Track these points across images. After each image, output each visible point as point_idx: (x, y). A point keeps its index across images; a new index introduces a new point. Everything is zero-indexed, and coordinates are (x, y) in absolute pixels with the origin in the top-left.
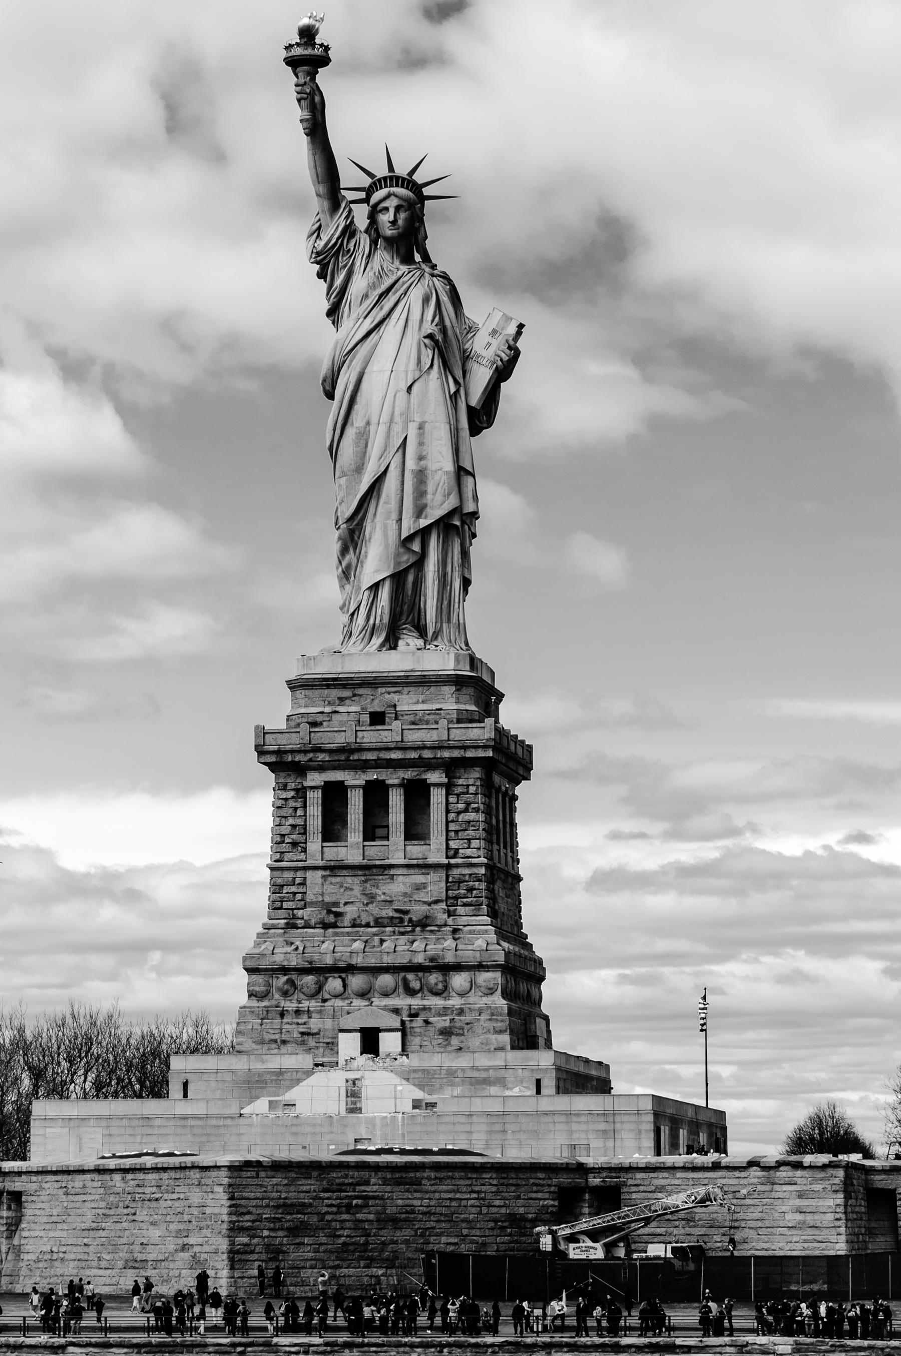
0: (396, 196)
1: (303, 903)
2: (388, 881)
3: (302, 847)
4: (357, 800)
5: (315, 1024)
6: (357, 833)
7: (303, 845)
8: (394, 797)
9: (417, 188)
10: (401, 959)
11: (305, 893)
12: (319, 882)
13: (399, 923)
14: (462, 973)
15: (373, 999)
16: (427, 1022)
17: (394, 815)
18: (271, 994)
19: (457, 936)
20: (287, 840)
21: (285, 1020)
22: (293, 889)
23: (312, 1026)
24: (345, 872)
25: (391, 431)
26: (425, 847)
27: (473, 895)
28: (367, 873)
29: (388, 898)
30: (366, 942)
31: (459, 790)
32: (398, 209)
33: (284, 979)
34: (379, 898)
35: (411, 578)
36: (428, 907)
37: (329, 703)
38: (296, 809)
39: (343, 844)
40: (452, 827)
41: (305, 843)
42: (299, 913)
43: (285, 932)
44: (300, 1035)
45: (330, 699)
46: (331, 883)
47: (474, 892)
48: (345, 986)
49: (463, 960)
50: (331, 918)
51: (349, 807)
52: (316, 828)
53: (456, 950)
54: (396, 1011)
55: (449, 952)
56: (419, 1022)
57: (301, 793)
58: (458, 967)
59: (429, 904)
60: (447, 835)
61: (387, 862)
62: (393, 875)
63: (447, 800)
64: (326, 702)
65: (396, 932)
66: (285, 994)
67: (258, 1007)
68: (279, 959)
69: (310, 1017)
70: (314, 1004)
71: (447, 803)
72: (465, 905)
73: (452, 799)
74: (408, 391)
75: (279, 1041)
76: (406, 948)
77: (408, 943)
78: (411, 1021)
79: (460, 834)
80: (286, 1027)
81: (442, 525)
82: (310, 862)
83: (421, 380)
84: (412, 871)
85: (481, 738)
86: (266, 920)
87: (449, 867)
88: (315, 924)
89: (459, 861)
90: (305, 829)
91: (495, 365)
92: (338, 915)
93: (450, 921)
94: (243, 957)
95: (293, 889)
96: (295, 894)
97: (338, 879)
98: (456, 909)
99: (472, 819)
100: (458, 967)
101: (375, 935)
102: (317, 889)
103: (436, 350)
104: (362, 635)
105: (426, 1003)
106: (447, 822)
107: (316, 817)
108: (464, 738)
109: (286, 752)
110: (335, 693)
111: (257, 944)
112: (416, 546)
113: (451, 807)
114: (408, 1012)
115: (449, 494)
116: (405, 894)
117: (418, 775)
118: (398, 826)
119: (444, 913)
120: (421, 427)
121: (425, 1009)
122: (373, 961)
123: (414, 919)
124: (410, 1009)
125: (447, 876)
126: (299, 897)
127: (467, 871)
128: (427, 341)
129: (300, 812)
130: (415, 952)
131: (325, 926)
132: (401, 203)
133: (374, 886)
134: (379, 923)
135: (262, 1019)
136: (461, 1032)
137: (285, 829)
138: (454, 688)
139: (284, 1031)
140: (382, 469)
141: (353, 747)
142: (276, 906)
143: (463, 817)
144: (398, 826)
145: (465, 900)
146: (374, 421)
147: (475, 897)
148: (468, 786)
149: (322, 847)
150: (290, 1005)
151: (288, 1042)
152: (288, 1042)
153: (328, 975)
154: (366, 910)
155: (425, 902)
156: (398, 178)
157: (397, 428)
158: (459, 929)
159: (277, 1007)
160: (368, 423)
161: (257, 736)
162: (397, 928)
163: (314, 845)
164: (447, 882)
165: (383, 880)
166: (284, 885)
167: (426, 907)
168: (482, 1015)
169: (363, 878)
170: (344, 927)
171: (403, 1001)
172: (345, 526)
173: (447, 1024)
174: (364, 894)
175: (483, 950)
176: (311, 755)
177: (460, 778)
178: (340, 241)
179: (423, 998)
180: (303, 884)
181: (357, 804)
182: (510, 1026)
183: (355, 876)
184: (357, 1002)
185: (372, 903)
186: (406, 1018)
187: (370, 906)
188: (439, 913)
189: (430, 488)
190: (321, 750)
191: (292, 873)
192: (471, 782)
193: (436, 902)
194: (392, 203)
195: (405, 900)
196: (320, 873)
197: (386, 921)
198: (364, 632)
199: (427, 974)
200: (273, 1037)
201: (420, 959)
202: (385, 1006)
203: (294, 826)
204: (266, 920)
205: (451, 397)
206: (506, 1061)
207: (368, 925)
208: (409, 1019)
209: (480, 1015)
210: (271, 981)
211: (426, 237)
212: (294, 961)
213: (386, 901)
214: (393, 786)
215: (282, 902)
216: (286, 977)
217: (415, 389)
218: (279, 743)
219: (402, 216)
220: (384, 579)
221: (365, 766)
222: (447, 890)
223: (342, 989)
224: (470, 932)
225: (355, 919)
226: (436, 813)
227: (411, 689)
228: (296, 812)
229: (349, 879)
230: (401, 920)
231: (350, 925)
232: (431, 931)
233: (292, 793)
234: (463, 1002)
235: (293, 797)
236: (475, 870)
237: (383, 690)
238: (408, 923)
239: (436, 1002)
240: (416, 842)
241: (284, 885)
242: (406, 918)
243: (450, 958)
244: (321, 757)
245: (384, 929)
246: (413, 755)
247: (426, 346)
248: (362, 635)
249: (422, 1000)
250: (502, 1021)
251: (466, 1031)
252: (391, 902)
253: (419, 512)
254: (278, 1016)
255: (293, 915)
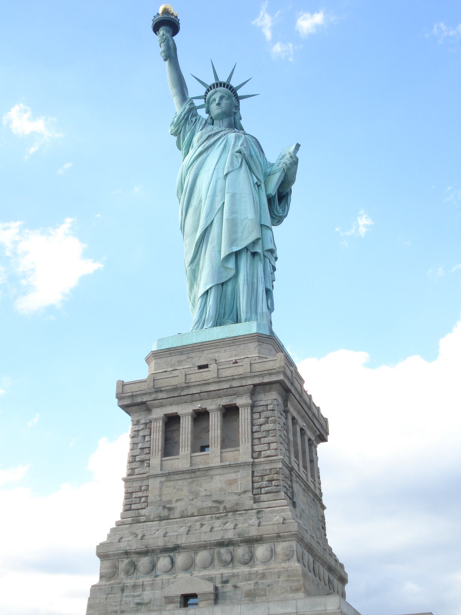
0: (220, 91)
1: (146, 504)
2: (209, 480)
3: (148, 463)
4: (187, 424)
5: (147, 595)
6: (186, 448)
7: (147, 461)
8: (213, 419)
9: (233, 91)
10: (216, 537)
11: (148, 496)
12: (158, 487)
13: (216, 511)
14: (264, 545)
15: (194, 572)
16: (235, 587)
17: (213, 431)
18: (116, 575)
19: (260, 516)
20: (138, 459)
21: (125, 594)
22: (140, 494)
23: (145, 598)
24: (177, 477)
25: (250, 300)
26: (236, 452)
27: (273, 485)
28: (193, 475)
29: (208, 493)
30: (190, 527)
31: (260, 409)
32: (221, 98)
33: (126, 561)
34: (202, 494)
35: (229, 288)
36: (238, 497)
37: (171, 365)
38: (144, 436)
39: (176, 457)
40: (256, 435)
41: (149, 460)
42: (143, 512)
43: (130, 526)
44: (135, 606)
45: (171, 363)
46: (167, 487)
47: (274, 482)
48: (173, 562)
49: (264, 533)
50: (166, 513)
51: (181, 430)
52: (157, 447)
53: (259, 526)
54: (211, 579)
55: (253, 527)
56: (229, 587)
57: (148, 424)
58: (259, 540)
59: (239, 495)
60: (252, 442)
61: (208, 466)
62: (212, 476)
63: (252, 417)
64: (169, 365)
65: (214, 518)
66: (127, 573)
67: (105, 585)
68: (123, 546)
69: (144, 590)
70: (147, 580)
71: (252, 419)
72: (267, 493)
73: (256, 416)
74: (224, 179)
75: (119, 611)
76: (220, 528)
77: (222, 525)
78: (223, 587)
79: (262, 440)
80: (124, 599)
81: (249, 253)
82: (152, 472)
83: (233, 173)
84: (226, 471)
85: (274, 368)
86: (119, 519)
87: (253, 464)
88: (154, 518)
89: (262, 460)
90: (150, 450)
91: (283, 168)
92: (170, 509)
93: (255, 506)
94: (97, 546)
95: (140, 494)
96: (140, 498)
97: (172, 483)
98: (260, 496)
99: (270, 429)
100: (259, 540)
101: (197, 521)
102: (156, 493)
103: (244, 160)
104: (197, 325)
105: (235, 571)
106: (253, 432)
107: (157, 440)
108: (262, 369)
109: (136, 396)
110: (175, 359)
111: (109, 536)
112: (231, 264)
113: (255, 422)
114: (220, 580)
115: (252, 231)
116: (221, 490)
117: (230, 401)
118: (216, 439)
119: (251, 500)
120: (233, 196)
121: (234, 576)
122: (194, 540)
123: (228, 506)
124: (222, 576)
125: (253, 472)
126: (143, 500)
127: (268, 467)
128: (238, 154)
129: (147, 439)
130: (227, 530)
131: (161, 519)
132: (223, 94)
133: (198, 485)
134: (201, 513)
135: (107, 594)
136: (263, 593)
137: (137, 452)
138: (256, 343)
139: (123, 602)
140: (209, 223)
141: (183, 386)
142: (128, 507)
143: (264, 428)
144: (216, 439)
145: (266, 489)
146: (203, 198)
147: (274, 486)
148: (267, 405)
149: (162, 461)
150: (129, 582)
151: (126, 611)
152: (126, 611)
153: (159, 556)
154: (191, 504)
155: (235, 493)
156: (221, 84)
157: (218, 199)
158: (262, 511)
159: (119, 583)
160: (201, 201)
161: (118, 387)
162: (214, 515)
163: (156, 460)
164: (253, 477)
165: (204, 480)
166: (133, 493)
167: (236, 497)
168: (281, 577)
169: (190, 480)
170: (175, 518)
171: (217, 572)
172: (189, 268)
173: (252, 587)
174: (191, 492)
175: (280, 523)
176: (154, 396)
177: (261, 401)
178: (186, 116)
179: (233, 568)
180: (147, 490)
181: (187, 427)
182: (303, 585)
183: (185, 479)
184: (181, 575)
185: (196, 498)
186: (219, 585)
187: (195, 500)
188: (247, 501)
189: (240, 229)
190: (161, 391)
191: (140, 482)
192: (269, 402)
193: (245, 492)
194: (217, 96)
195: (221, 493)
196: (158, 480)
197: (206, 511)
198: (198, 323)
199: (236, 548)
200: (114, 609)
201: (230, 535)
202: (202, 576)
203: (142, 449)
204: (119, 519)
205: (254, 185)
206: (297, 608)
207: (193, 515)
208: (221, 585)
209: (279, 577)
210: (117, 564)
211: (241, 119)
212: (135, 545)
213: (207, 496)
214: (213, 410)
215: (131, 504)
216: (129, 560)
217: (229, 176)
218: (133, 390)
219: (224, 102)
220: (211, 288)
221: (193, 398)
222: (253, 482)
223: (170, 566)
224: (271, 512)
225: (183, 512)
226: (243, 426)
227: (227, 348)
228: (144, 439)
229: (180, 483)
230: (218, 508)
231: (179, 517)
232: (240, 514)
233: (142, 427)
234: (265, 568)
235: (143, 429)
236: (273, 466)
237: (208, 352)
238: (223, 510)
239: (245, 569)
240: (229, 450)
241: (133, 493)
242: (222, 507)
243: (254, 532)
244: (161, 395)
245: (204, 516)
246: (226, 385)
247: (237, 157)
248: (197, 325)
249: (232, 569)
250: (297, 581)
251: (267, 592)
252: (210, 495)
253: (232, 241)
254: (120, 591)
255: (139, 513)
